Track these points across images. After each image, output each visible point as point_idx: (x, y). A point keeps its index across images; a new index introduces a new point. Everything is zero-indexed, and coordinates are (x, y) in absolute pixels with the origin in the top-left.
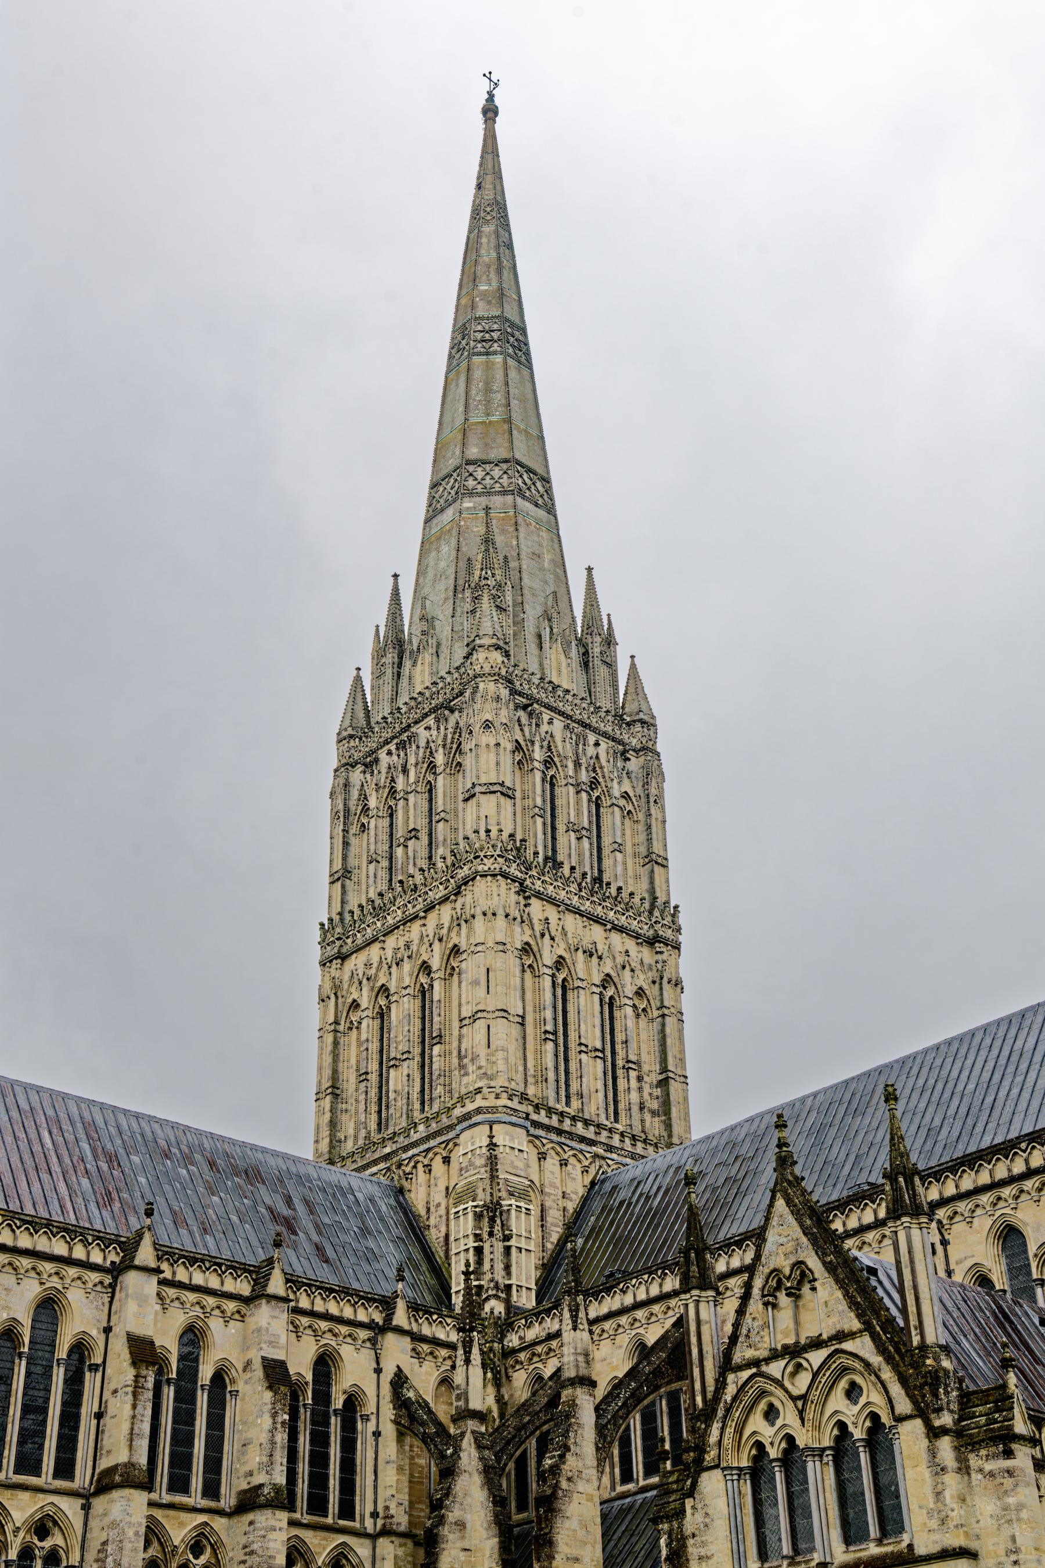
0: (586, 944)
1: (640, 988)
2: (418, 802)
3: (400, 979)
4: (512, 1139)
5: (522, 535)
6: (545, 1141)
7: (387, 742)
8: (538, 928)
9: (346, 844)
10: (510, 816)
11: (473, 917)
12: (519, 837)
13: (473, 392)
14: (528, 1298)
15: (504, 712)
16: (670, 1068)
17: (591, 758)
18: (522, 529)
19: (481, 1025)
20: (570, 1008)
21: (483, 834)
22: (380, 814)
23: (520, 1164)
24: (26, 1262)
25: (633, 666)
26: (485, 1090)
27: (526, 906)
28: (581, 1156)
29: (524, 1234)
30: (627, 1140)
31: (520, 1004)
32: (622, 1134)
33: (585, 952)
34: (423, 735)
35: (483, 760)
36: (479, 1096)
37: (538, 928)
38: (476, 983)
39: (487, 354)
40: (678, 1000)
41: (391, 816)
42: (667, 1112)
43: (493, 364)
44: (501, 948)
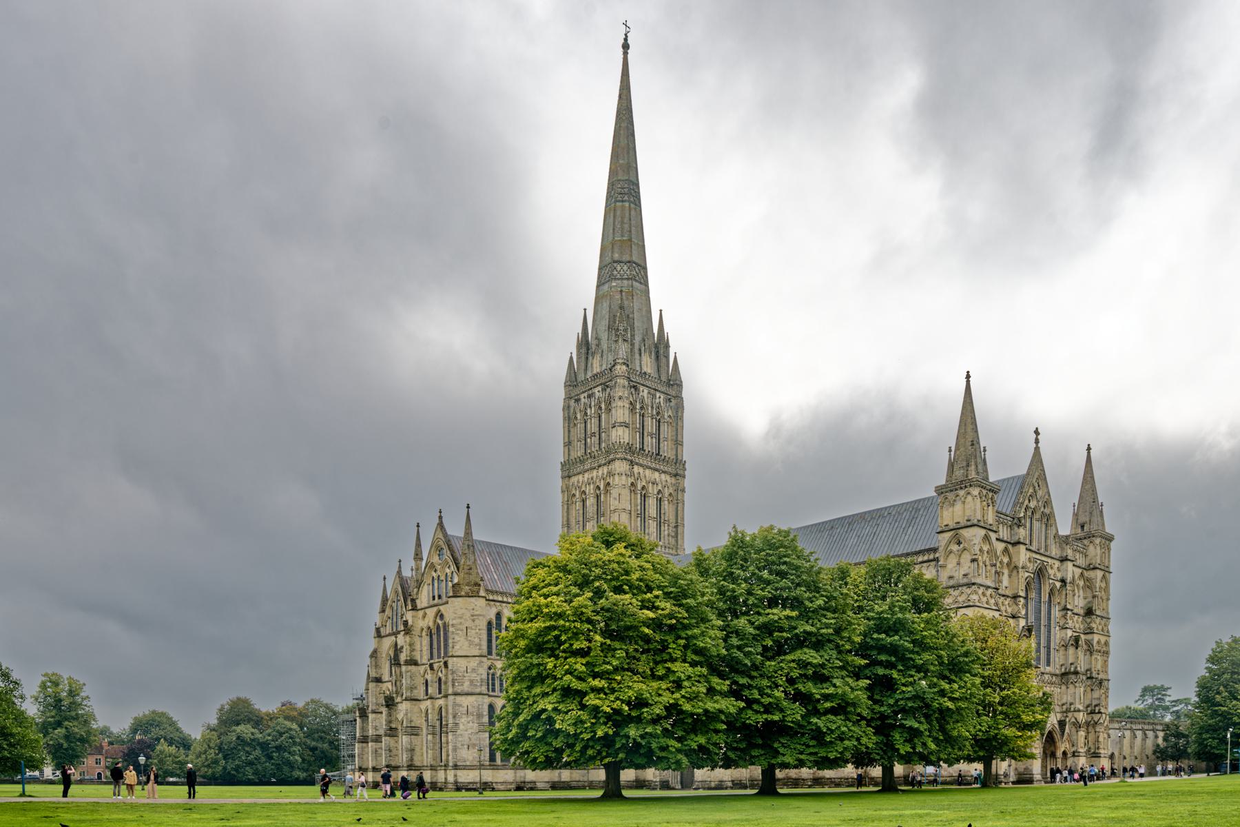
2: (595, 421)
3: (590, 490)
7: (583, 392)
9: (569, 431)
10: (627, 435)
12: (630, 443)
15: (626, 392)
16: (679, 522)
19: (617, 514)
21: (618, 441)
24: (492, 603)
25: (675, 357)
31: (629, 506)
34: (597, 394)
37: (636, 476)
38: (615, 499)
40: (683, 496)
41: (585, 423)
42: (677, 537)
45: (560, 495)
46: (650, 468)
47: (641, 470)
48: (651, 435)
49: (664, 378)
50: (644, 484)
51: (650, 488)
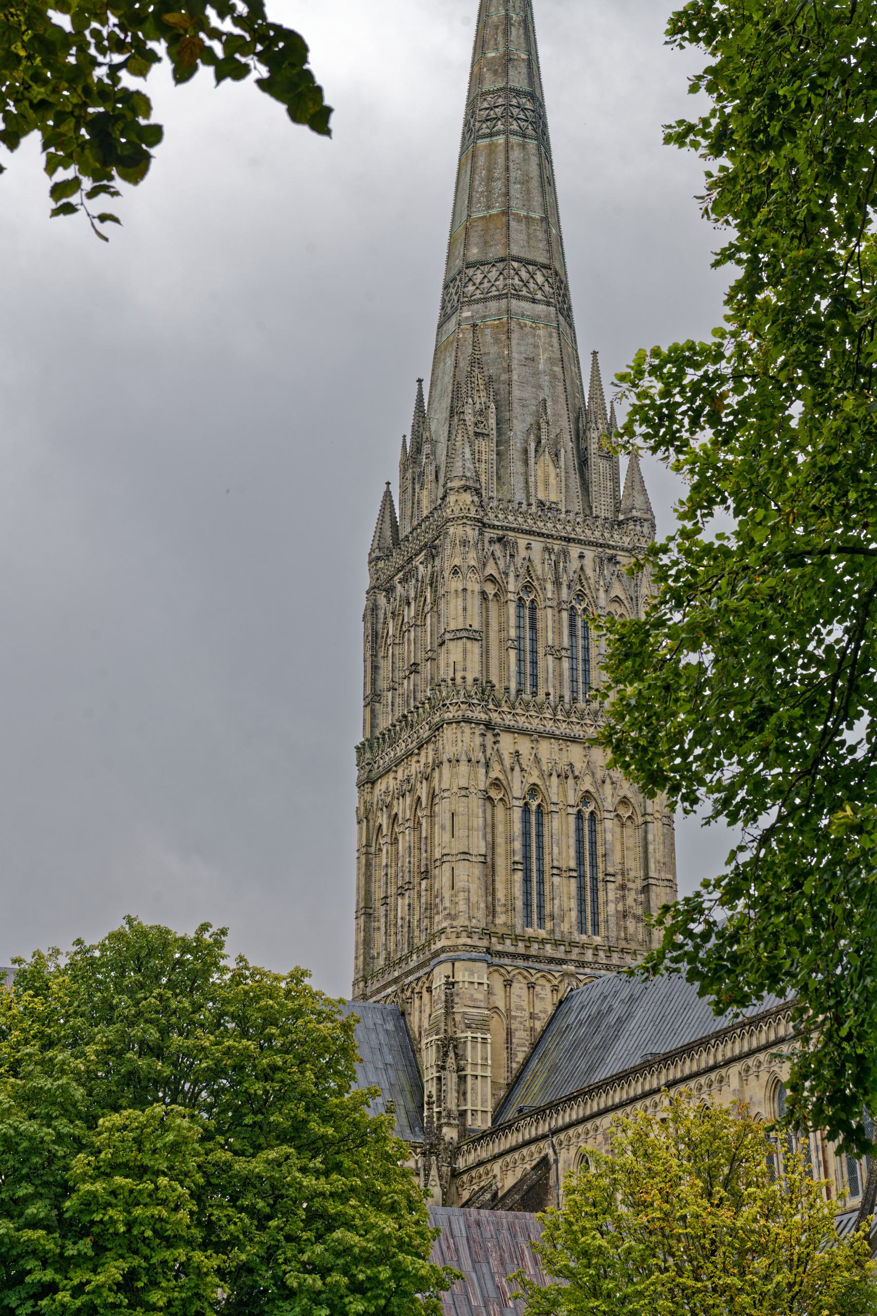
0: (562, 766)
1: (625, 797)
4: (472, 973)
5: (514, 342)
6: (509, 968)
8: (508, 761)
11: (441, 763)
13: (477, 183)
14: (484, 1121)
17: (575, 572)
18: (515, 336)
19: (446, 867)
20: (546, 832)
22: (397, 641)
23: (480, 996)
26: (449, 930)
27: (495, 743)
28: (550, 977)
29: (480, 1062)
30: (601, 954)
32: (596, 949)
33: (559, 776)
35: (452, 606)
36: (443, 936)
37: (508, 761)
39: (491, 135)
43: (496, 146)
44: (463, 792)
45: (356, 827)
46: (553, 736)
47: (524, 746)
48: (556, 653)
49: (602, 508)
50: (534, 779)
51: (554, 790)
